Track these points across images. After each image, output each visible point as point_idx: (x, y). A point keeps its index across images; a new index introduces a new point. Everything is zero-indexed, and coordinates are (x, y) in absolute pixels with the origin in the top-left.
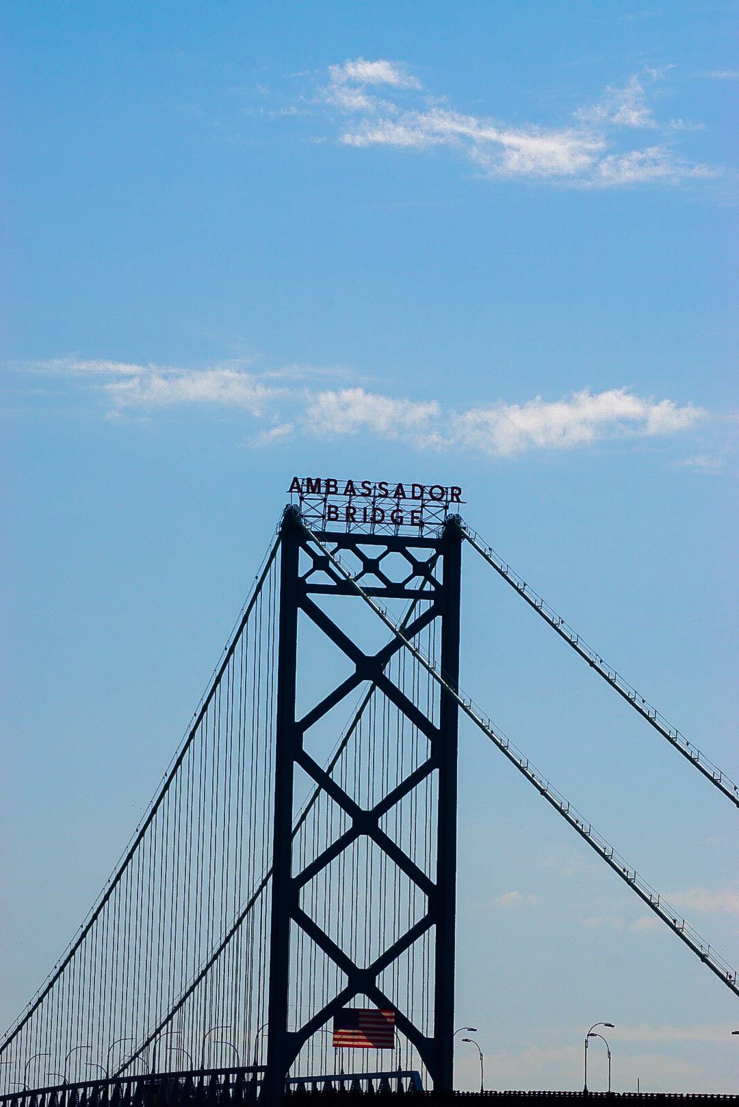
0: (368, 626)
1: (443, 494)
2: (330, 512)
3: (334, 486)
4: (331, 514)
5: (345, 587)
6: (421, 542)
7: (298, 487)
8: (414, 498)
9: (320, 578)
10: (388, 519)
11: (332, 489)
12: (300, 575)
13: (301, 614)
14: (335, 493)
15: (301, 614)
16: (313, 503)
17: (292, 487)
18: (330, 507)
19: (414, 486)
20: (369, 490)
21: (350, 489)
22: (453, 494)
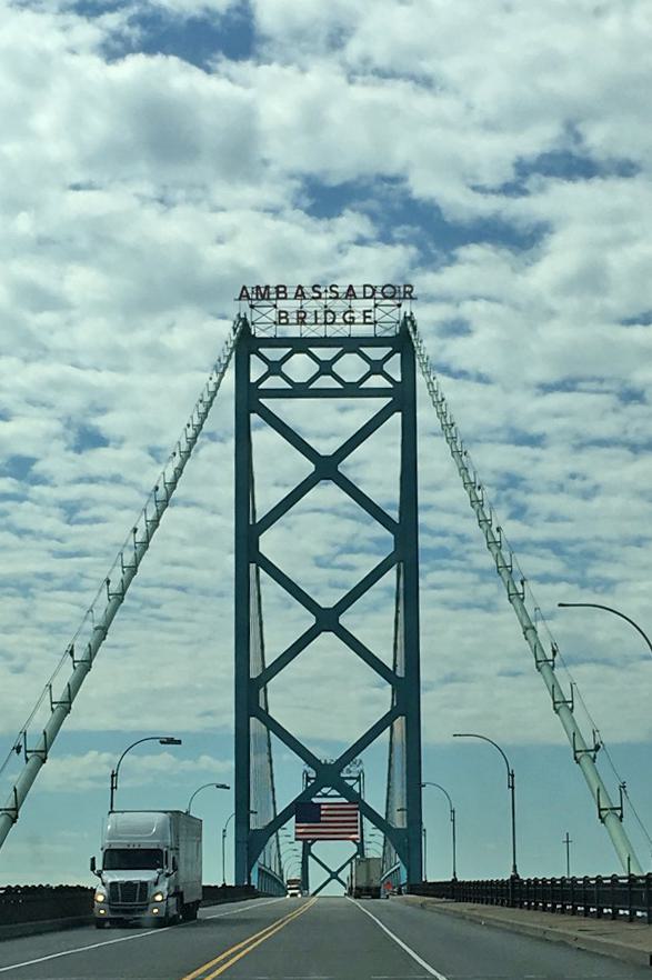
0: (326, 422)
1: (395, 293)
2: (280, 318)
3: (284, 292)
4: (282, 319)
5: (300, 391)
6: (375, 341)
7: (247, 295)
8: (365, 298)
9: (275, 382)
10: (339, 320)
11: (281, 295)
12: (253, 379)
13: (310, 858)
14: (285, 298)
15: (310, 858)
16: (265, 310)
17: (241, 295)
18: (280, 312)
19: (365, 286)
20: (320, 293)
21: (300, 293)
22: (405, 292)
